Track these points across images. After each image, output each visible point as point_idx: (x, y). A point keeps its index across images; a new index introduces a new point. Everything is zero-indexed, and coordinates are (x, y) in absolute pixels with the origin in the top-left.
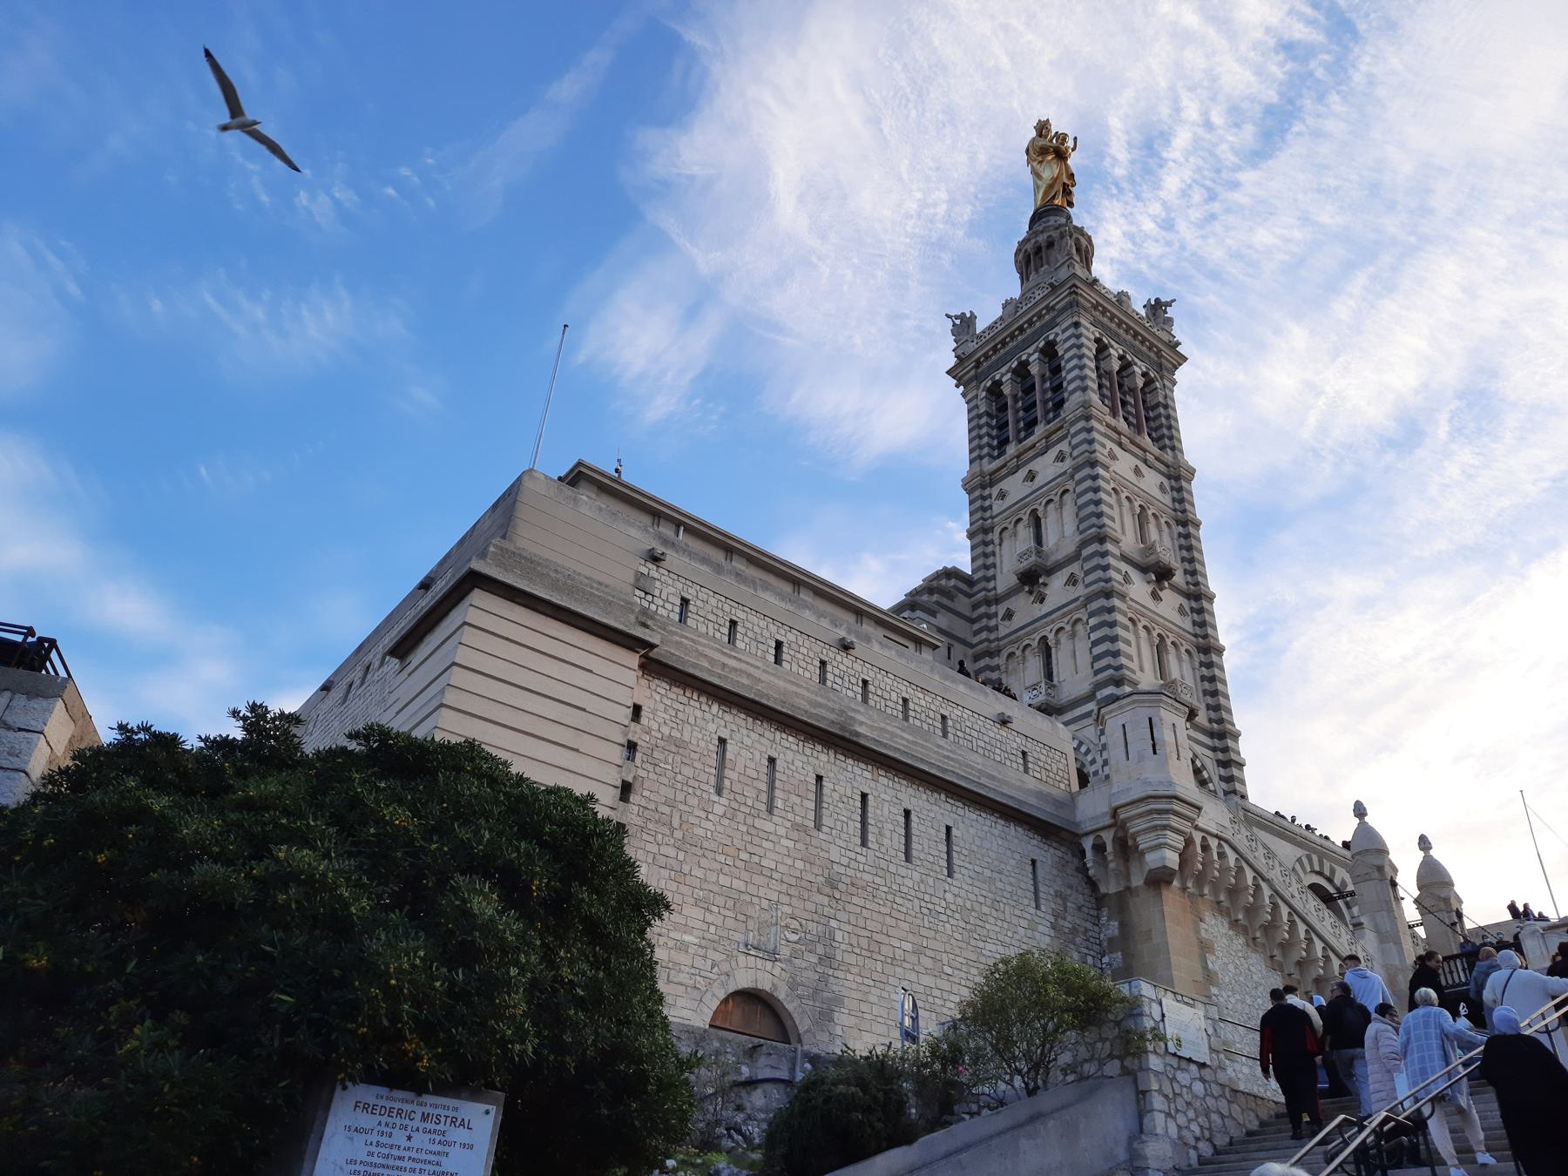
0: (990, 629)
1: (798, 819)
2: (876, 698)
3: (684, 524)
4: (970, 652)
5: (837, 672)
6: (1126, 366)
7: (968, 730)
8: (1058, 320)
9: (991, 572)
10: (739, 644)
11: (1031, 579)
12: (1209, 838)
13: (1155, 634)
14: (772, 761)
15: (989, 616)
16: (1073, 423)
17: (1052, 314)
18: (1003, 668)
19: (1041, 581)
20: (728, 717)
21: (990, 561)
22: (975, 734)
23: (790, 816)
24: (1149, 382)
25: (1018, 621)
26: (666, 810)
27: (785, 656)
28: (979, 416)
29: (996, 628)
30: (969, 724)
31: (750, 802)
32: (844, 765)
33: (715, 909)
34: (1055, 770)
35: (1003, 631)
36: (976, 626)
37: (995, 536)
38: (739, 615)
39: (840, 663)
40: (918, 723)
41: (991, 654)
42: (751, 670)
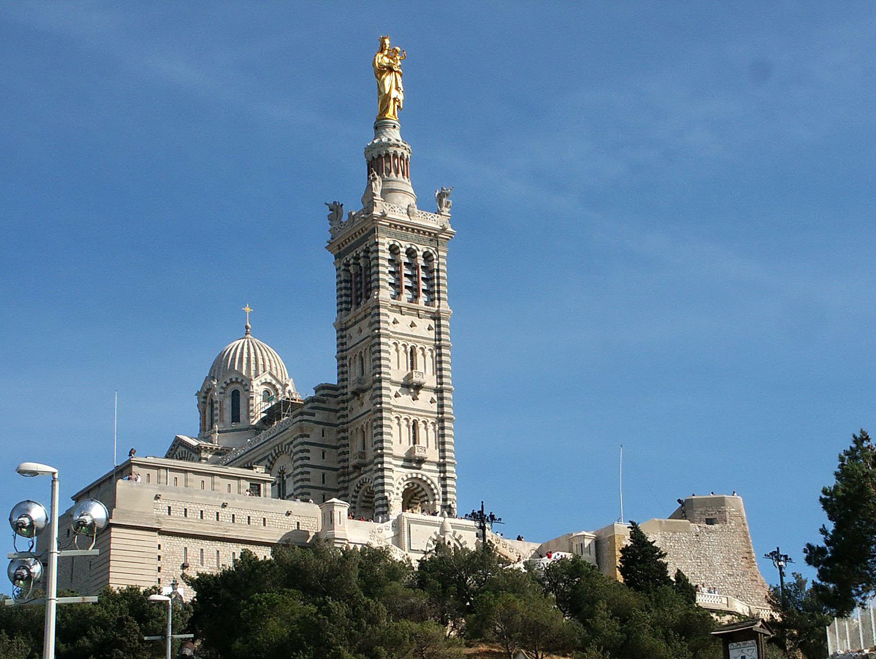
0: (343, 416)
1: (211, 566)
2: (238, 519)
3: (170, 468)
4: (335, 429)
5: (223, 515)
6: (411, 253)
7: (274, 521)
9: (345, 383)
10: (188, 516)
11: (356, 393)
12: (357, 545)
13: (411, 421)
14: (202, 550)
15: (344, 409)
16: (373, 309)
17: (366, 232)
18: (349, 438)
19: (361, 396)
20: (187, 540)
21: (345, 376)
22: (277, 521)
23: (209, 565)
24: (427, 256)
25: (355, 414)
26: (171, 572)
27: (204, 515)
28: (341, 282)
29: (347, 416)
30: (275, 518)
31: (196, 564)
32: (226, 545)
33: (188, 595)
34: (311, 525)
35: (350, 418)
36: (338, 415)
37: (347, 362)
38: (187, 506)
39: (224, 512)
40: (254, 524)
41: (344, 431)
42: (193, 524)
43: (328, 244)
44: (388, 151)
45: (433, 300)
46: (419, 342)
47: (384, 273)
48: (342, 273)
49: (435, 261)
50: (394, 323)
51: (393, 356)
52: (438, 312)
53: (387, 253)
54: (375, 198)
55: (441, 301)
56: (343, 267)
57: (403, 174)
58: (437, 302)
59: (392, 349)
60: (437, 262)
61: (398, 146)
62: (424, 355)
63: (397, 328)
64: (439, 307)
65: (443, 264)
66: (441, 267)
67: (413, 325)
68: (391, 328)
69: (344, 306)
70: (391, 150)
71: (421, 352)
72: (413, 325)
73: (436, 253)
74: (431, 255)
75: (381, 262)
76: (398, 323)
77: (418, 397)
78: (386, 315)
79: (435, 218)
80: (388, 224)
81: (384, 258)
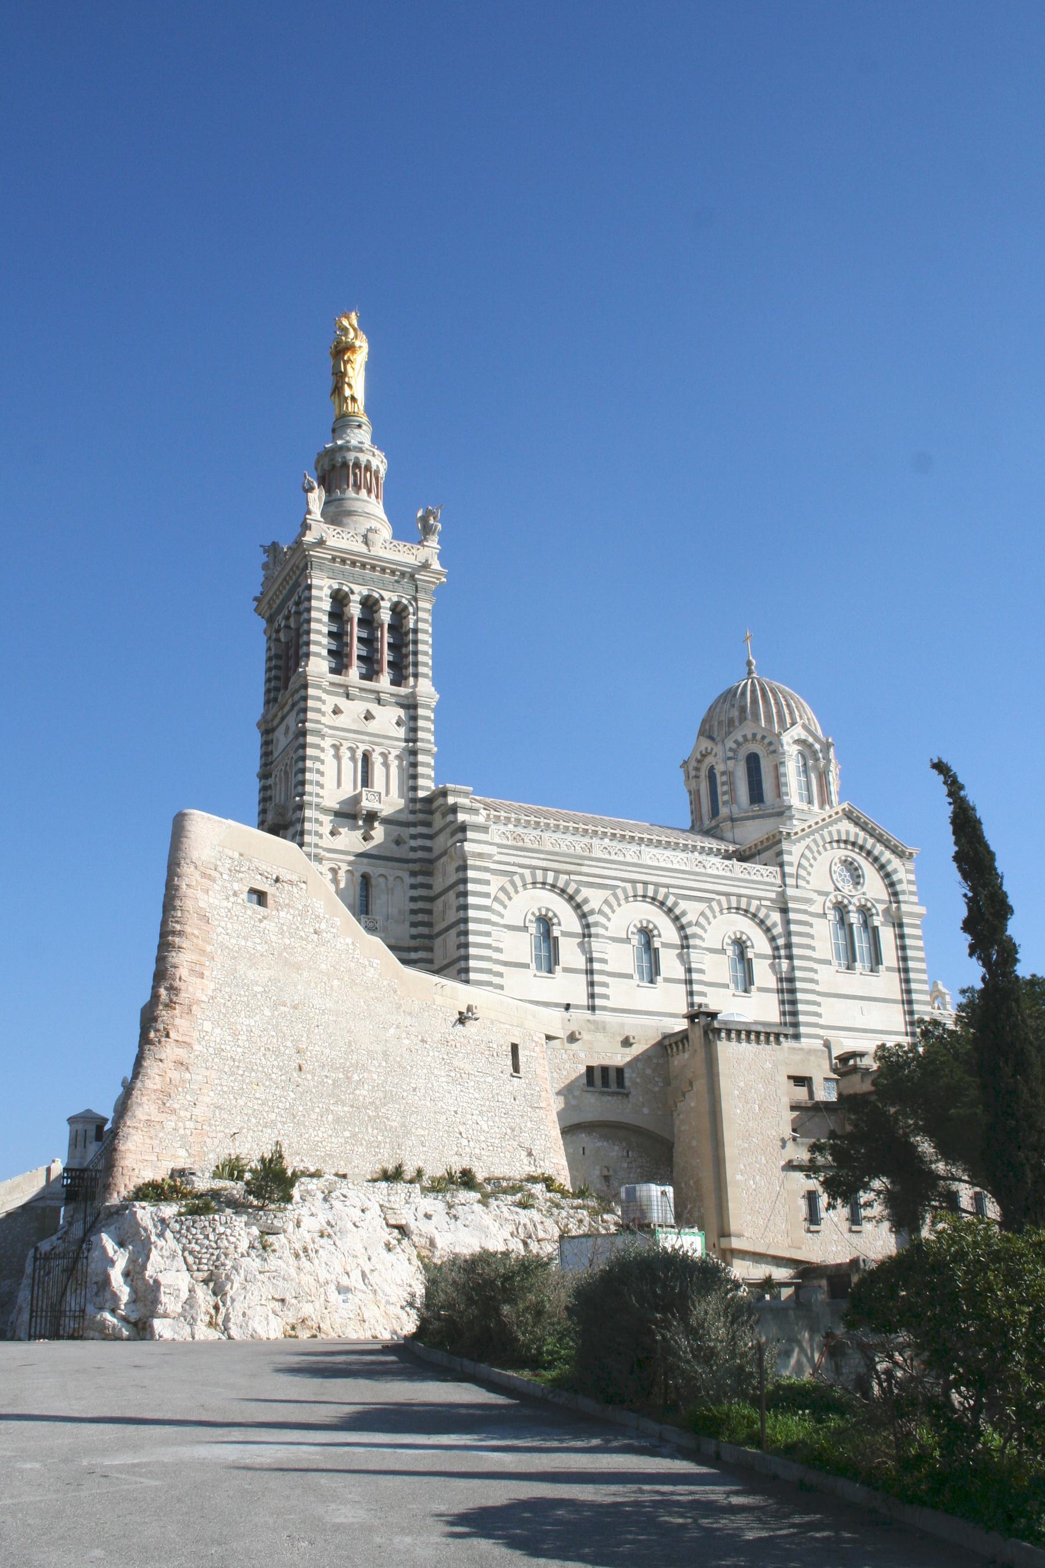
6: (370, 605)
8: (300, 580)
37: (270, 781)
43: (256, 603)
44: (345, 457)
45: (406, 678)
46: (378, 744)
47: (319, 632)
48: (272, 645)
49: (411, 616)
50: (336, 711)
51: (329, 766)
52: (413, 695)
53: (326, 601)
54: (308, 516)
55: (419, 678)
56: (274, 636)
57: (369, 491)
58: (411, 680)
59: (328, 756)
60: (415, 617)
61: (361, 450)
62: (386, 765)
63: (341, 721)
64: (415, 686)
65: (425, 621)
66: (421, 625)
67: (369, 716)
68: (329, 719)
69: (272, 695)
70: (351, 456)
71: (380, 760)
72: (369, 716)
73: (414, 604)
74: (406, 608)
75: (314, 614)
76: (342, 712)
77: (372, 833)
78: (319, 699)
79: (414, 551)
80: (330, 557)
81: (319, 610)
